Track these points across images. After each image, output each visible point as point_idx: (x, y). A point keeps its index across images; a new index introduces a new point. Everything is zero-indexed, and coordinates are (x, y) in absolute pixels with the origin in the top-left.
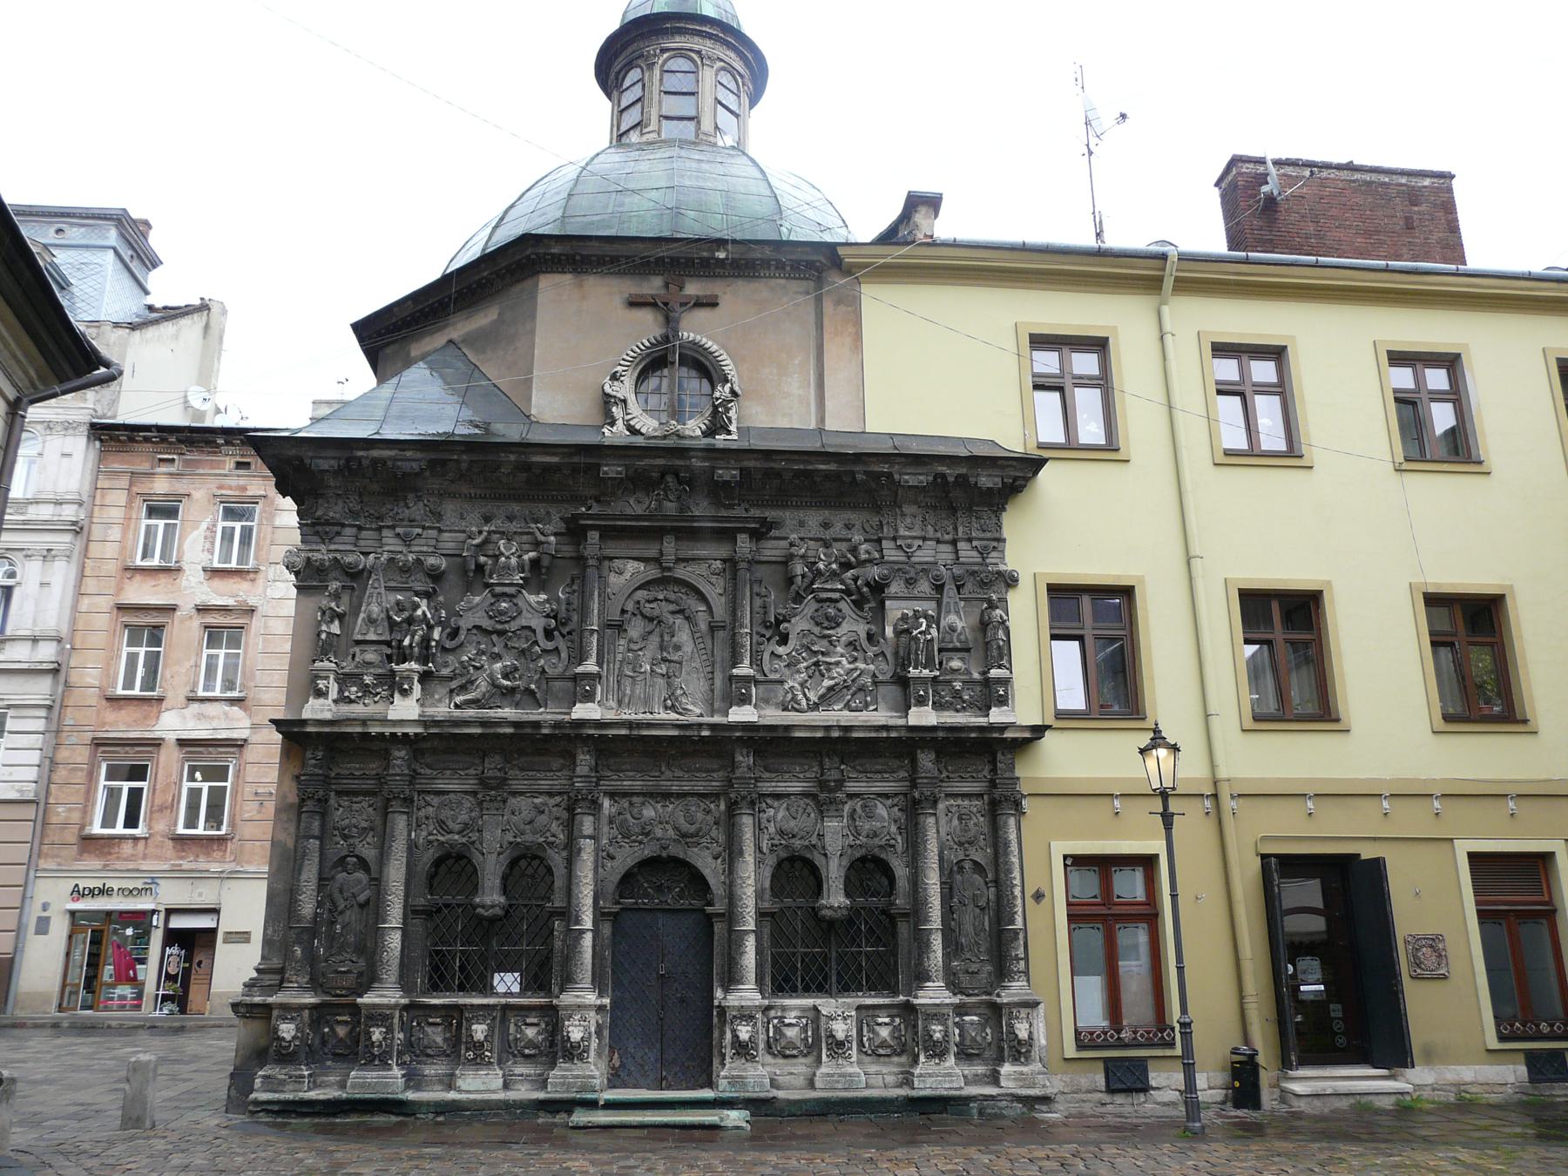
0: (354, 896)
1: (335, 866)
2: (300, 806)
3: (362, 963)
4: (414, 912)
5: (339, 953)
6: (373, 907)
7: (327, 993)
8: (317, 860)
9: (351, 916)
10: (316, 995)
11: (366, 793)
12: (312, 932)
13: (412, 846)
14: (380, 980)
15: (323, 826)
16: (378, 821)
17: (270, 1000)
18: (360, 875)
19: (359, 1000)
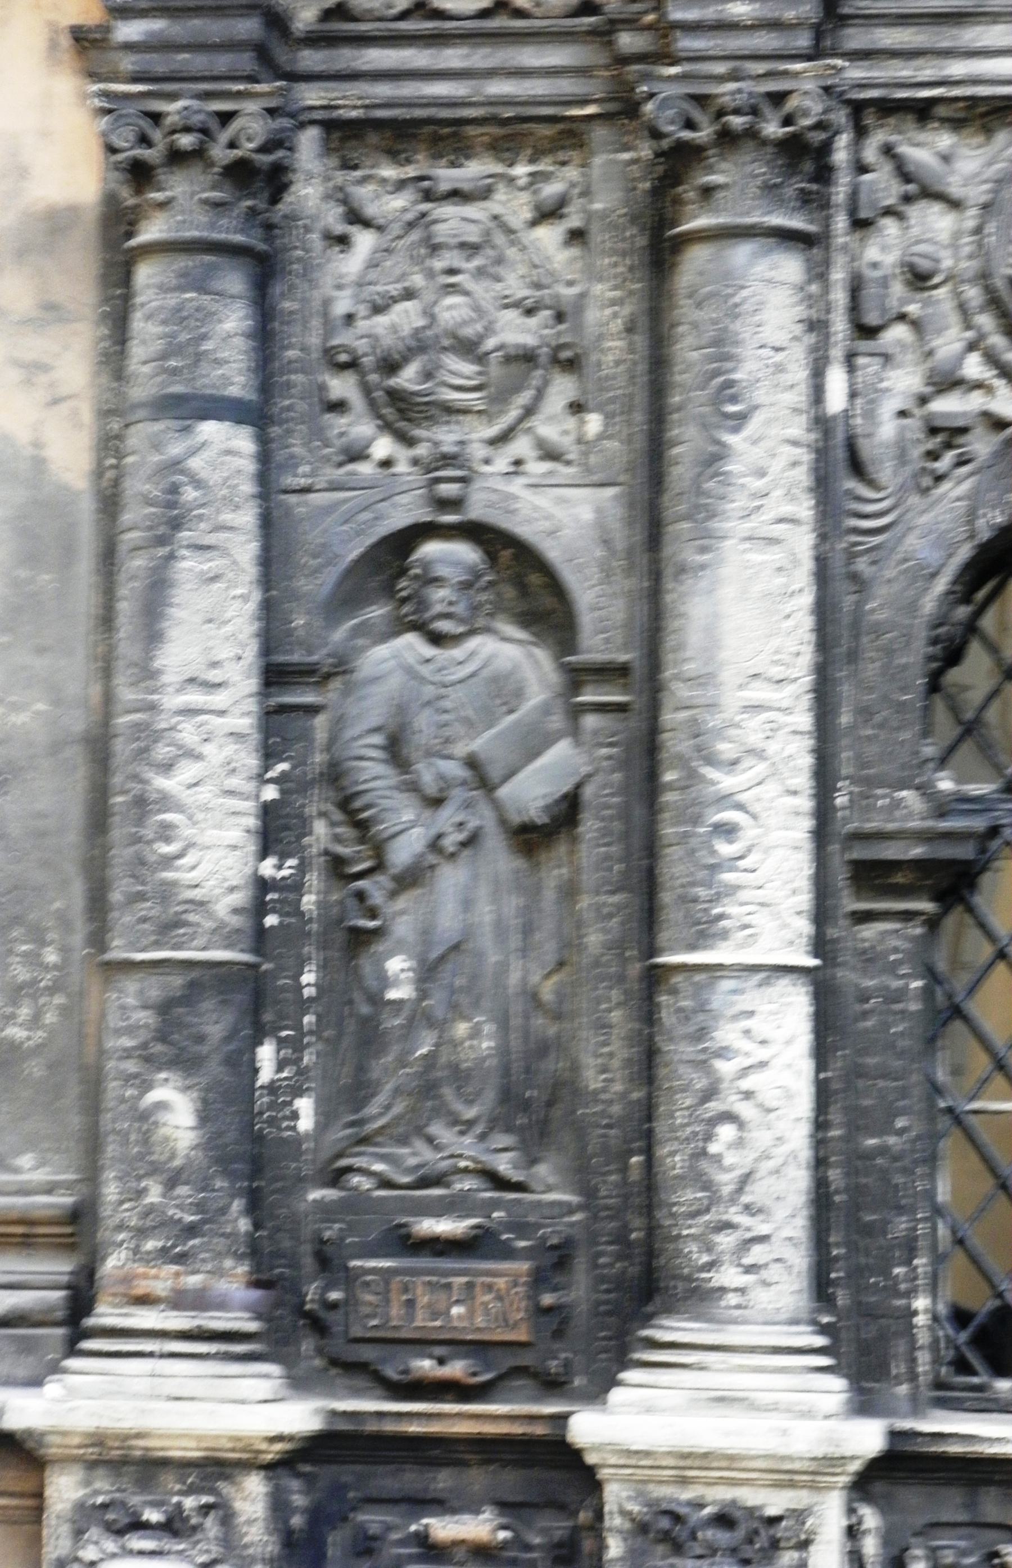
0: (481, 777)
1: (348, 597)
2: (117, 222)
3: (551, 1186)
4: (872, 876)
5: (412, 1129)
6: (625, 839)
7: (353, 1369)
8: (246, 550)
9: (469, 900)
10: (299, 1383)
11: (513, 132)
12: (252, 995)
13: (839, 459)
14: (699, 1298)
15: (266, 335)
16: (606, 314)
17: (25, 1410)
18: (505, 650)
19: (588, 1428)
